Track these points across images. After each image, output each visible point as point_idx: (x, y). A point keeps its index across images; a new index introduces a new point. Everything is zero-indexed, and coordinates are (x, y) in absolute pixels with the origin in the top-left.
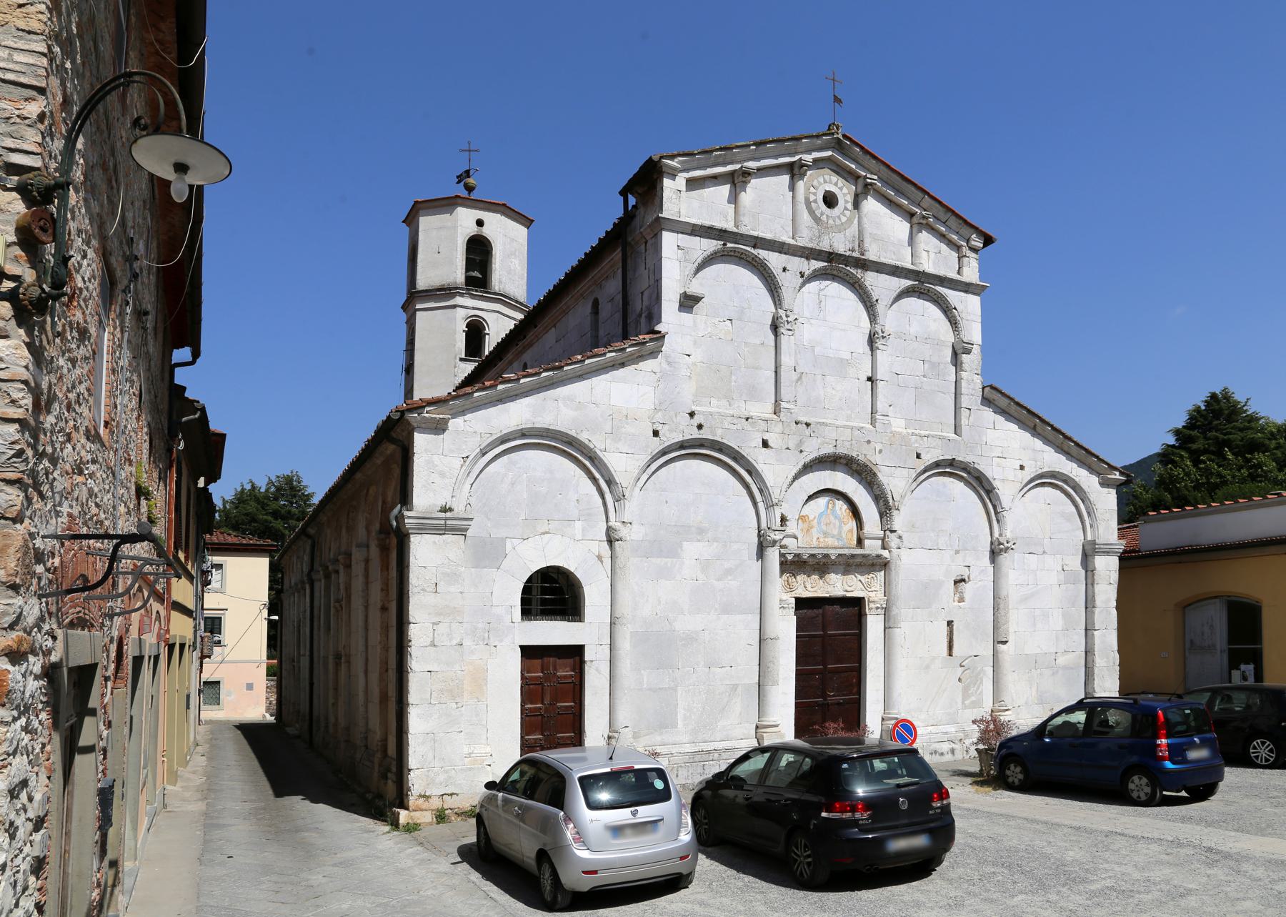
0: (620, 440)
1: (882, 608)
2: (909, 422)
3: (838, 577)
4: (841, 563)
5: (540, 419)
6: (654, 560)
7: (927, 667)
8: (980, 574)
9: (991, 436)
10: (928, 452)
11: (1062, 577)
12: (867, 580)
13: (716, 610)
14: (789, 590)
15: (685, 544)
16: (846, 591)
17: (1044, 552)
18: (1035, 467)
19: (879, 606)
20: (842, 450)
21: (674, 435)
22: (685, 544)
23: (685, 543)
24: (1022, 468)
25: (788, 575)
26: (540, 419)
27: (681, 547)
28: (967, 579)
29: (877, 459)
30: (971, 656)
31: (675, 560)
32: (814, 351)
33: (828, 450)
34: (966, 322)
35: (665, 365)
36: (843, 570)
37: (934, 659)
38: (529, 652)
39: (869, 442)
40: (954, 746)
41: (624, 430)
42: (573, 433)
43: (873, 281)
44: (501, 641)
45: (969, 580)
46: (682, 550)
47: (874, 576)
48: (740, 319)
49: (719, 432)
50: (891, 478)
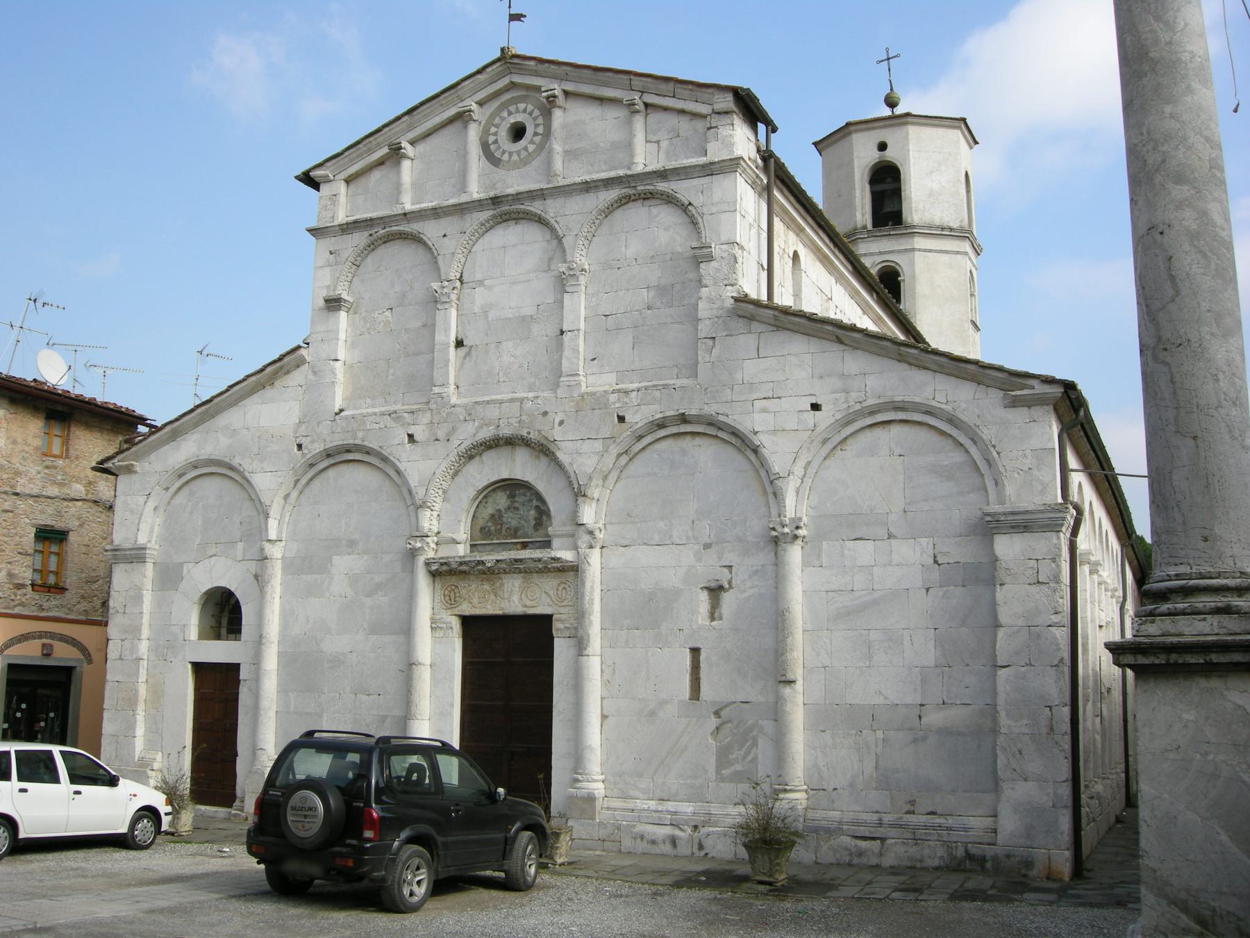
0: (265, 459)
2: (622, 375)
5: (203, 451)
6: (304, 577)
7: (652, 714)
8: (751, 577)
9: (751, 369)
10: (637, 411)
11: (935, 575)
13: (365, 629)
14: (449, 606)
15: (335, 558)
16: (526, 606)
17: (890, 536)
18: (847, 401)
19: (567, 625)
20: (506, 431)
21: (316, 445)
22: (335, 558)
23: (335, 557)
24: (815, 407)
26: (203, 451)
27: (331, 562)
28: (727, 586)
29: (557, 434)
30: (734, 702)
31: (324, 576)
32: (487, 317)
33: (486, 433)
34: (710, 217)
35: (311, 377)
37: (664, 702)
38: (198, 668)
39: (545, 413)
40: (678, 833)
41: (269, 449)
42: (227, 460)
43: (550, 209)
44: (175, 657)
45: (731, 587)
46: (331, 565)
48: (401, 305)
49: (360, 434)
50: (575, 455)
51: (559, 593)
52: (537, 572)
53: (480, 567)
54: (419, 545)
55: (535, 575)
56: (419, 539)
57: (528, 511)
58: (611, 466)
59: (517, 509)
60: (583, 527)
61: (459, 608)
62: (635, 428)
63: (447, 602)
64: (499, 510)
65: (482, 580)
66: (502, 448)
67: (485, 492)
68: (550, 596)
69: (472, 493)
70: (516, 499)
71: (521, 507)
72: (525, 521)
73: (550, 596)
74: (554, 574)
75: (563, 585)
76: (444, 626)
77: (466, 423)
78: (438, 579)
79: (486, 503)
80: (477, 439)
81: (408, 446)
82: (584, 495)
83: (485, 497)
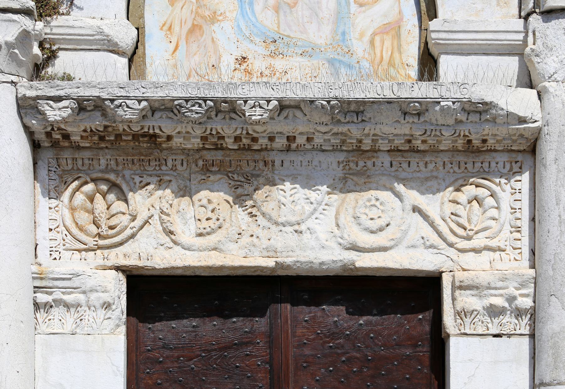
1: (519, 313)
3: (313, 195)
4: (318, 140)
12: (449, 208)
14: (91, 242)
16: (354, 248)
19: (499, 302)
25: (90, 187)
36: (339, 173)
47: (482, 192)
63: (81, 229)
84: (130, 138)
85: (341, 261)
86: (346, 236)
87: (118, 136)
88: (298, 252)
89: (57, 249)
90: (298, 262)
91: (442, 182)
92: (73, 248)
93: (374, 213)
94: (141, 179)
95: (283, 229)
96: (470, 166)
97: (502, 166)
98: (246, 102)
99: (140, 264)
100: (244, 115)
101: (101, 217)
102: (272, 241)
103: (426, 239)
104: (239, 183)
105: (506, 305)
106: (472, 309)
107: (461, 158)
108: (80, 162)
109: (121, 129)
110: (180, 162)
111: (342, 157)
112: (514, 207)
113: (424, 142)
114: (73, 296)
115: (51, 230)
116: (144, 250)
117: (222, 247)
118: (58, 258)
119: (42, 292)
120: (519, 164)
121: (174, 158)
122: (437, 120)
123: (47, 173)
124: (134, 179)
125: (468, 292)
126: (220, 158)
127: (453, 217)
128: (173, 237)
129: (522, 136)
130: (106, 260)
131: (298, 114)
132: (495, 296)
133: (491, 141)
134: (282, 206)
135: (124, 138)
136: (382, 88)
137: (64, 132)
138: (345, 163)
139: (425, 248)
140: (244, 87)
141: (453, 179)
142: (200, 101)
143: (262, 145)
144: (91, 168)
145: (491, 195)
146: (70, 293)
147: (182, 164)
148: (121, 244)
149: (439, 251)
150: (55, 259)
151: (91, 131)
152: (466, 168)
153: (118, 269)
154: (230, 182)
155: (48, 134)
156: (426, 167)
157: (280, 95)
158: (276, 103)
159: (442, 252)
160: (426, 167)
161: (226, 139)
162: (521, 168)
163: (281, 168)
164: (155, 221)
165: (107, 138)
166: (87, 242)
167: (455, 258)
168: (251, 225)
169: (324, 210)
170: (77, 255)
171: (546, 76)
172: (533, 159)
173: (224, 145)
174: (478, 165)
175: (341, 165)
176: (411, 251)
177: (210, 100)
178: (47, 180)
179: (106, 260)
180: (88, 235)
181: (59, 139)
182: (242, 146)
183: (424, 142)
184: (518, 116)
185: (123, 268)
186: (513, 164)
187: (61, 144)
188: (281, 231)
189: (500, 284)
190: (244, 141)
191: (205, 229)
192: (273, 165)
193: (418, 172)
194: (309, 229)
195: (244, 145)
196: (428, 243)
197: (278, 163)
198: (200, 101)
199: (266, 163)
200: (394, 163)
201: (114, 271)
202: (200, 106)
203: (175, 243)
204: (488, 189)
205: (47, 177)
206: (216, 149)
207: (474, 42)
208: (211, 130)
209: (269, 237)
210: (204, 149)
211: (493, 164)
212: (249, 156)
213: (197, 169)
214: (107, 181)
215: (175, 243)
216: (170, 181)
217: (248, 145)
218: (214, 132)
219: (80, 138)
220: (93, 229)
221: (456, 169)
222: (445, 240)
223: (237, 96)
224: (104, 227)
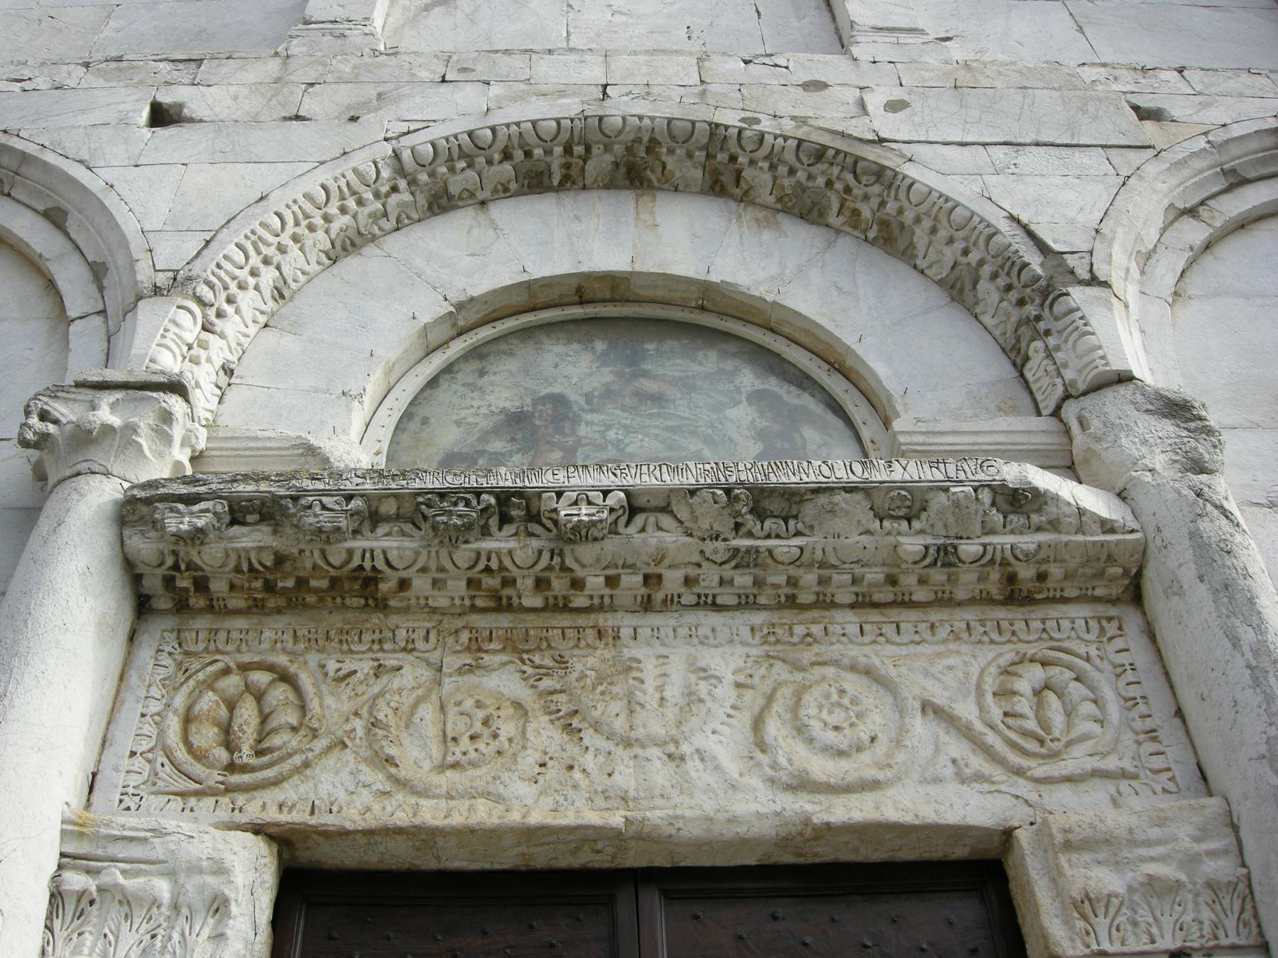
14: (214, 777)
29: (888, 125)
51: (1024, 705)
52: (863, 603)
53: (501, 542)
54: (106, 413)
55: (848, 621)
56: (119, 395)
57: (716, 408)
58: (1155, 236)
59: (657, 399)
60: (1124, 391)
61: (288, 792)
62: (1221, 136)
63: (199, 755)
64: (559, 401)
65: (476, 646)
66: (583, 195)
67: (486, 333)
68: (966, 732)
69: (431, 308)
70: (647, 366)
71: (672, 393)
72: (707, 440)
73: (966, 732)
74: (970, 614)
75: (1036, 674)
76: (163, 888)
77: (444, 88)
78: (157, 631)
79: (482, 373)
80: (497, 119)
81: (147, 133)
82: (1094, 281)
83: (476, 353)
84: (324, 584)
85: (777, 814)
86: (783, 761)
87: (302, 583)
88: (676, 798)
89: (136, 792)
90: (676, 817)
91: (973, 661)
92: (172, 789)
93: (837, 717)
94: (339, 665)
95: (639, 751)
96: (1019, 625)
97: (1084, 628)
98: (559, 494)
99: (313, 821)
100: (556, 522)
101: (244, 732)
102: (616, 776)
103: (962, 763)
104: (542, 671)
105: (1183, 877)
106: (1105, 892)
107: (1001, 613)
108: (222, 636)
109: (309, 564)
110: (422, 633)
111: (758, 618)
112: (1132, 695)
113: (922, 581)
114: (141, 880)
115: (133, 754)
116: (325, 797)
117: (501, 789)
118: (133, 807)
119: (75, 868)
120: (1115, 624)
121: (411, 625)
122: (945, 526)
123: (153, 653)
124: (323, 666)
125: (1087, 857)
126: (506, 625)
127: (1010, 721)
128: (393, 770)
129: (1111, 559)
130: (237, 811)
131: (666, 520)
132: (1152, 859)
133: (1056, 571)
134: (638, 709)
135: (314, 583)
136: (832, 469)
137: (200, 574)
138: (765, 631)
139: (963, 782)
140: (556, 472)
141: (991, 655)
142: (468, 496)
143: (591, 597)
144: (244, 647)
145: (1077, 679)
146: (138, 873)
147: (427, 639)
148: (276, 782)
149: (994, 788)
150: (128, 809)
151: (252, 569)
152: (1014, 633)
153: (258, 830)
154: (525, 668)
155: (169, 581)
156: (933, 635)
157: (629, 481)
158: (622, 494)
159: (1003, 788)
160: (933, 635)
161: (519, 581)
162: (1120, 628)
163: (632, 643)
164: (357, 741)
165: (280, 584)
166: (203, 776)
167: (1033, 797)
168: (568, 747)
169: (729, 716)
170: (177, 803)
171: (1128, 462)
172: (1139, 614)
173: (515, 601)
174: (1036, 625)
175: (758, 635)
176: (932, 790)
177: (487, 492)
178: (150, 666)
179: (237, 811)
180: (211, 766)
181: (186, 590)
182: (551, 601)
183: (922, 581)
184: (1100, 517)
185: (272, 830)
186: (1104, 623)
187: (192, 601)
188: (636, 757)
189: (1154, 833)
190: (556, 583)
191: (465, 754)
192: (617, 637)
193: (918, 643)
194: (698, 751)
195: (556, 598)
196: (968, 771)
197: (626, 632)
198: (468, 496)
199: (600, 634)
200: (866, 627)
201: (249, 836)
202: (468, 504)
203: (397, 781)
204: (1069, 667)
205: (152, 662)
206: (499, 609)
207: (976, 447)
208: (489, 559)
209: (609, 769)
210: (474, 609)
211: (1065, 624)
212: (565, 620)
213: (459, 648)
214: (270, 668)
215: (397, 781)
216: (400, 668)
217: (565, 598)
218: (494, 565)
219: (226, 588)
220: (222, 755)
221: (995, 636)
222: (1001, 762)
223: (541, 485)
224: (246, 749)
